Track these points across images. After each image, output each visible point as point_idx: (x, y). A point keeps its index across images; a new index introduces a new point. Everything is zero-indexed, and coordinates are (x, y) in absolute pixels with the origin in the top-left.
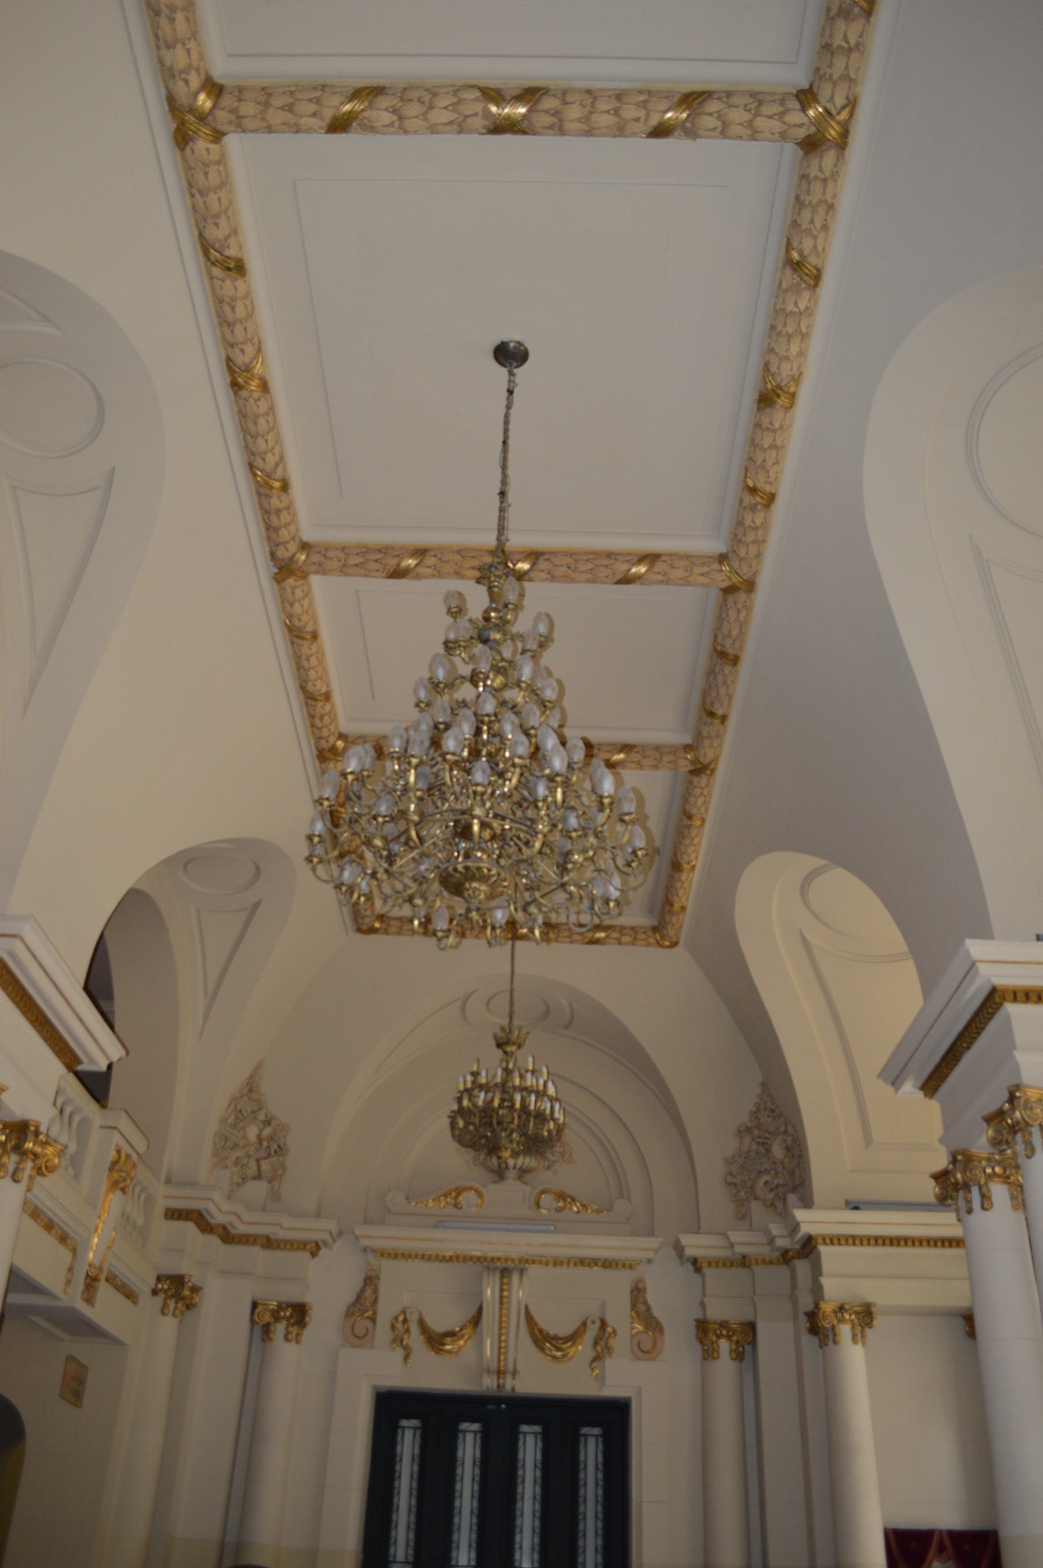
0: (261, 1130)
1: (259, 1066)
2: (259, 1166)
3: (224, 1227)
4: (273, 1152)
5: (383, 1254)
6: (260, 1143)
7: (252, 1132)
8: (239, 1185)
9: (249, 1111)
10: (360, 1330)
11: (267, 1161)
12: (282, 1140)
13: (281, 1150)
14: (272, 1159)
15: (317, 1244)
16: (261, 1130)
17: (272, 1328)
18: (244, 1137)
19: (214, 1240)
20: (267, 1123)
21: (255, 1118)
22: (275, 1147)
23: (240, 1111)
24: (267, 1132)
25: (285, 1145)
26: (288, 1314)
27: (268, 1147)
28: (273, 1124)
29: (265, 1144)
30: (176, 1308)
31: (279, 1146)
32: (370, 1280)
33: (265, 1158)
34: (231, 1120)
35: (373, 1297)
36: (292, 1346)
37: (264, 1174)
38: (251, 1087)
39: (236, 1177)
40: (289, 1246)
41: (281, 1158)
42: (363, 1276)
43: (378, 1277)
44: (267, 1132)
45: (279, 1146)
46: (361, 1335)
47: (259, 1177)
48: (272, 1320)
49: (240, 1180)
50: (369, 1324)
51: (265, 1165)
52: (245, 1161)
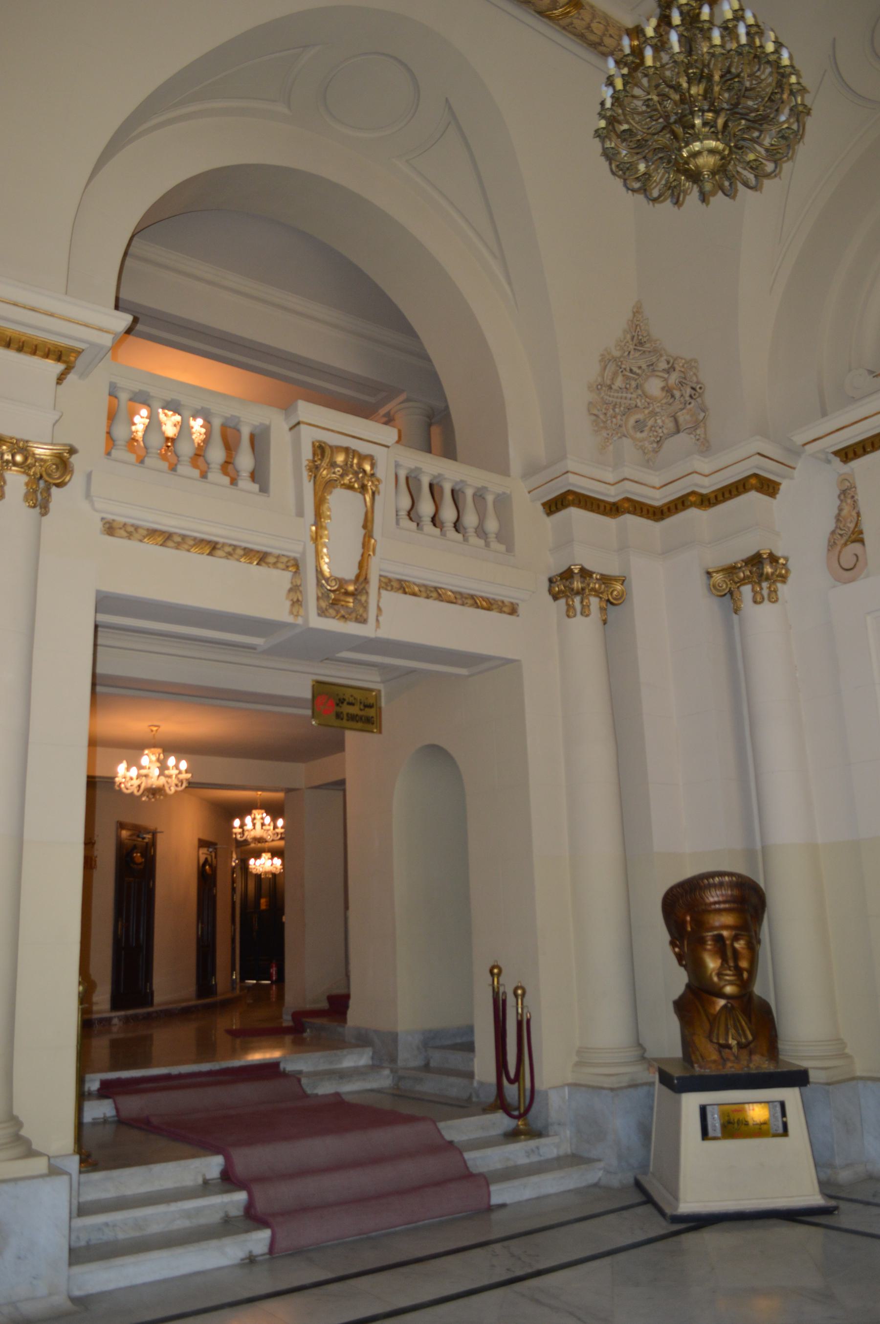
0: (666, 380)
1: (637, 311)
2: (676, 421)
3: (627, 499)
4: (688, 398)
5: (848, 454)
6: (673, 396)
7: (654, 387)
8: (656, 451)
9: (644, 366)
10: (847, 559)
11: (684, 411)
12: (695, 379)
13: (696, 392)
14: (688, 407)
15: (755, 475)
16: (666, 380)
17: (736, 594)
18: (645, 395)
19: (631, 520)
20: (672, 369)
21: (654, 371)
22: (689, 391)
23: (631, 371)
24: (674, 378)
25: (698, 383)
26: (748, 573)
27: (682, 395)
28: (678, 368)
29: (677, 394)
30: (583, 607)
31: (693, 389)
32: (847, 493)
33: (682, 409)
34: (619, 382)
35: (854, 513)
36: (766, 606)
37: (682, 428)
38: (639, 339)
39: (646, 444)
40: (727, 495)
41: (699, 400)
42: (838, 492)
43: (853, 487)
44: (674, 378)
45: (693, 389)
46: (851, 566)
47: (678, 431)
48: (733, 587)
49: (655, 445)
50: (857, 546)
51: (683, 417)
52: (650, 423)
